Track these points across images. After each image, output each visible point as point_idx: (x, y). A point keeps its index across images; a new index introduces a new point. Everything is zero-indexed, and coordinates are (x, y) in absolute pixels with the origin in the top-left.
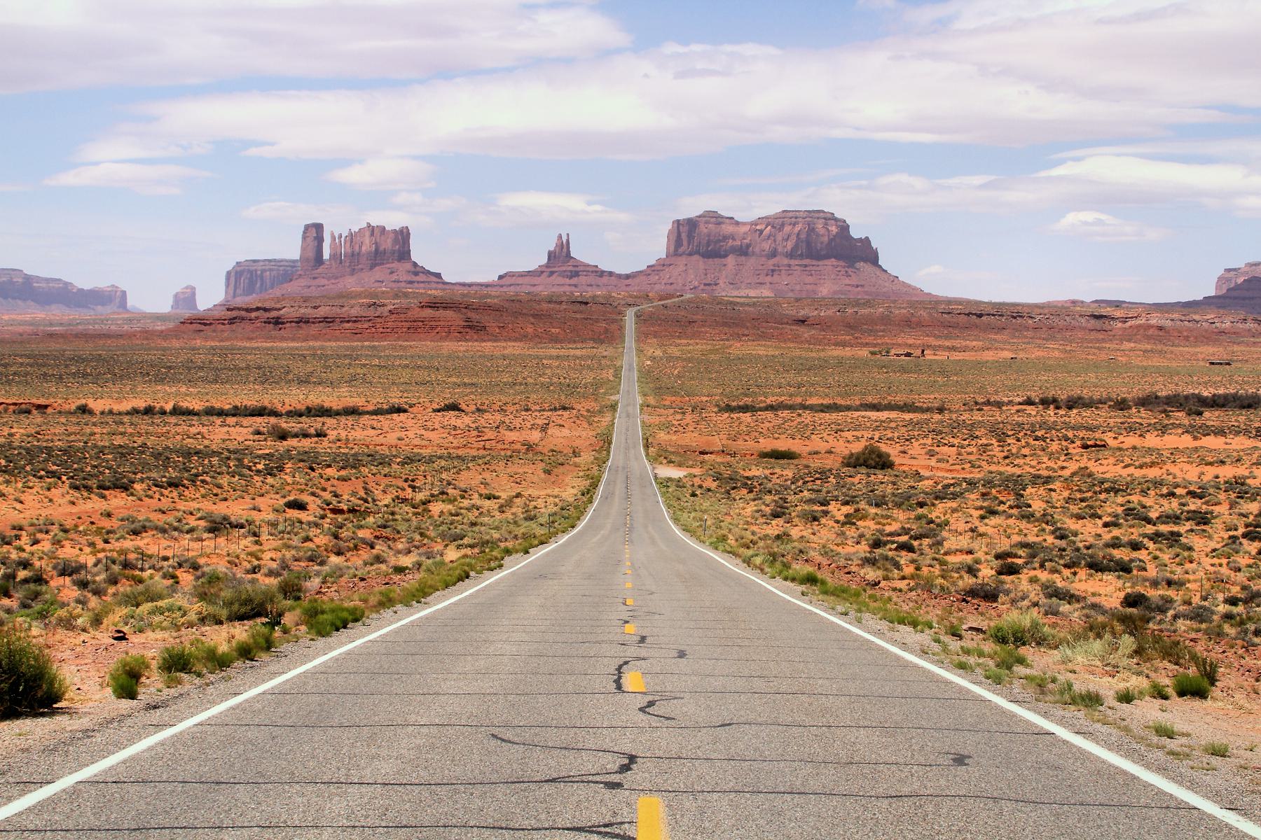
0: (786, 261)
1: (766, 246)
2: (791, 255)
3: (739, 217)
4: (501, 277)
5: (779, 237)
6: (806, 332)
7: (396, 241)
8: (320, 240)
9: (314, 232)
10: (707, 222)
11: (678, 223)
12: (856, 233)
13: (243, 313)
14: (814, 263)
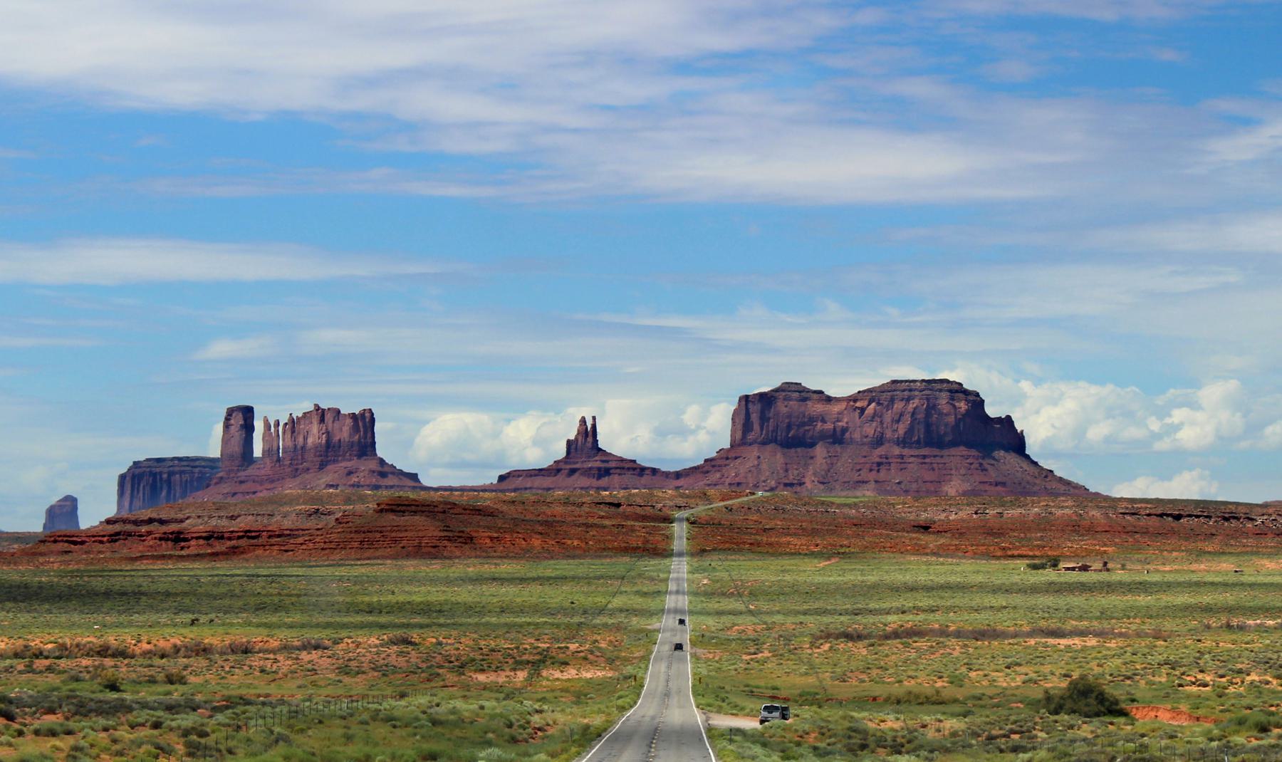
0: (897, 451)
1: (870, 430)
2: (903, 442)
3: (832, 392)
4: (502, 478)
5: (888, 417)
6: (930, 541)
7: (355, 428)
8: (249, 428)
10: (787, 399)
11: (746, 399)
12: (992, 411)
13: (129, 527)
14: (936, 451)
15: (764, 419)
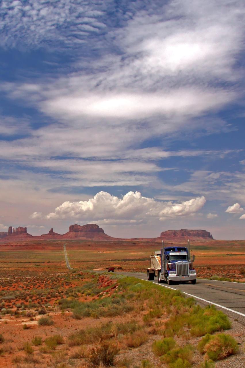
4: (41, 235)
8: (12, 229)
9: (10, 228)
10: (76, 226)
11: (71, 226)
15: (73, 228)
